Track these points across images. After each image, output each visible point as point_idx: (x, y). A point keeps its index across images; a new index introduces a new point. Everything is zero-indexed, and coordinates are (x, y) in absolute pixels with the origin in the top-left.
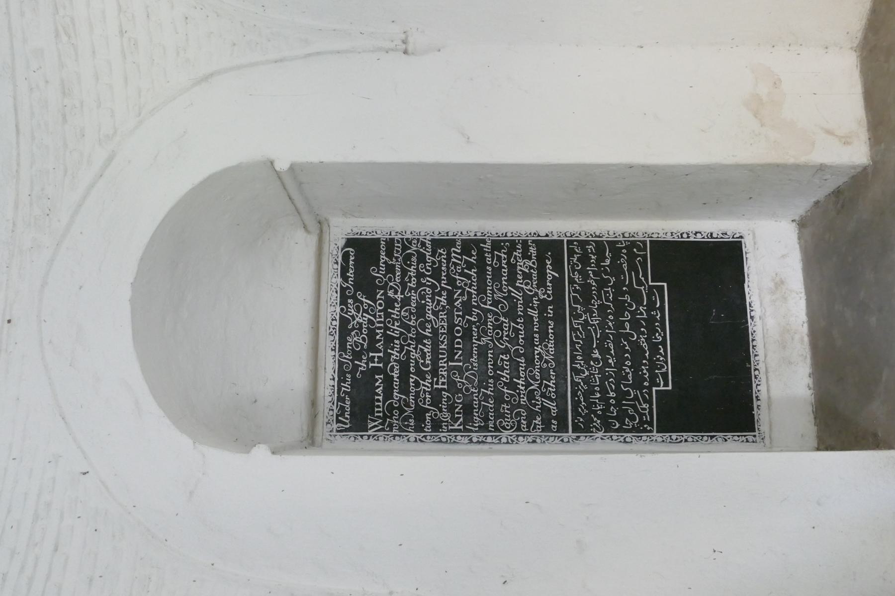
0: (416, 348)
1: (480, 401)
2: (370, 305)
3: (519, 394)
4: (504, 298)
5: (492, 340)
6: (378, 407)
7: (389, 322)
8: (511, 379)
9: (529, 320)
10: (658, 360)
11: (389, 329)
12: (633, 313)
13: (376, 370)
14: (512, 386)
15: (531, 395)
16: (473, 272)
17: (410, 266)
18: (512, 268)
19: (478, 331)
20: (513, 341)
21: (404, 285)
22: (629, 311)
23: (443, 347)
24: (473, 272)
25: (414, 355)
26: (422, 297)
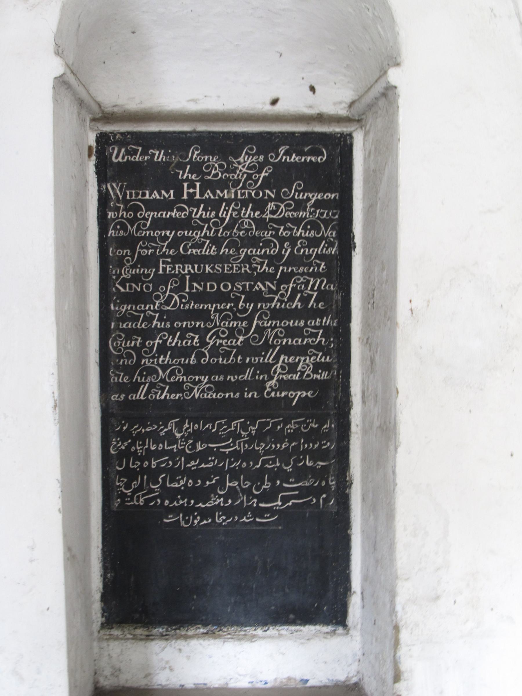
0: (205, 237)
1: (144, 312)
2: (256, 182)
3: (153, 357)
4: (267, 341)
5: (215, 326)
6: (137, 194)
7: (237, 205)
8: (171, 348)
9: (240, 369)
10: (195, 518)
11: (228, 205)
12: (248, 492)
13: (179, 193)
14: (163, 349)
15: (152, 371)
16: (297, 304)
17: (305, 229)
18: (302, 351)
19: (226, 310)
20: (215, 351)
21: (282, 221)
22: (251, 487)
23: (208, 269)
24: (297, 304)
25: (197, 235)
26: (267, 244)
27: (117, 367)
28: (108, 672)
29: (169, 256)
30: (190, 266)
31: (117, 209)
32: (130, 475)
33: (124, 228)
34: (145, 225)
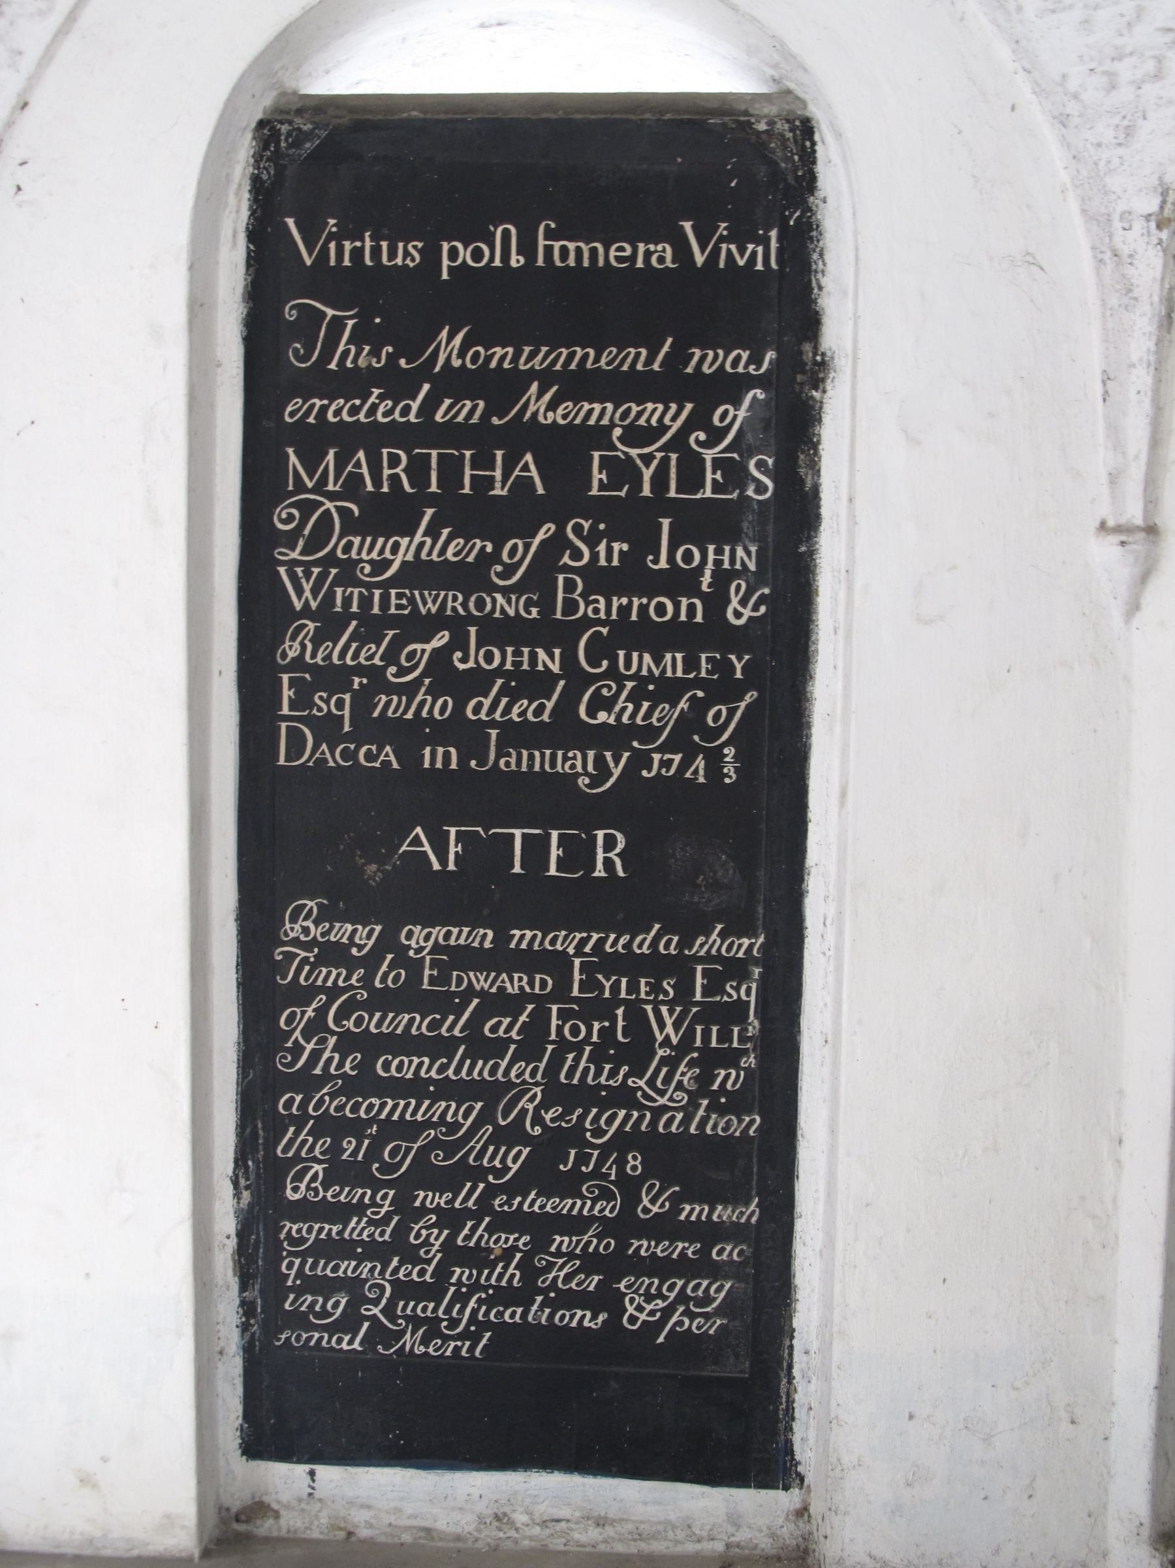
30: (525, 978)
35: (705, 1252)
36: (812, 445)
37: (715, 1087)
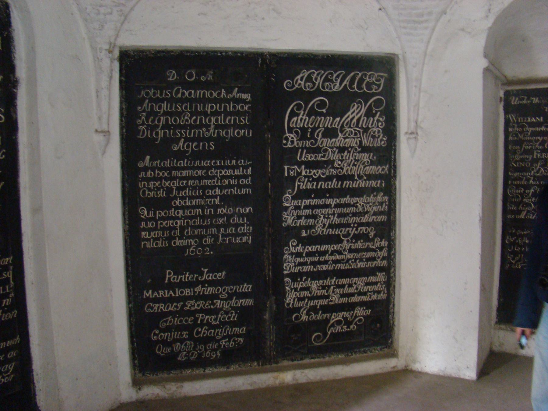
3: (529, 198)
6: (524, 119)
27: (511, 202)
28: (497, 344)
29: (540, 149)
31: (513, 127)
32: (515, 254)
33: (517, 135)
34: (527, 134)
35: (6, 357)
36: (15, 106)
37: (3, 305)
